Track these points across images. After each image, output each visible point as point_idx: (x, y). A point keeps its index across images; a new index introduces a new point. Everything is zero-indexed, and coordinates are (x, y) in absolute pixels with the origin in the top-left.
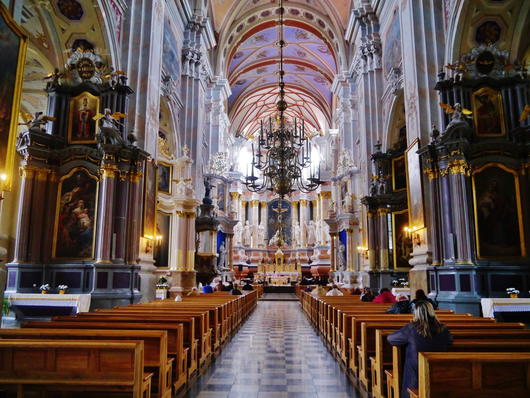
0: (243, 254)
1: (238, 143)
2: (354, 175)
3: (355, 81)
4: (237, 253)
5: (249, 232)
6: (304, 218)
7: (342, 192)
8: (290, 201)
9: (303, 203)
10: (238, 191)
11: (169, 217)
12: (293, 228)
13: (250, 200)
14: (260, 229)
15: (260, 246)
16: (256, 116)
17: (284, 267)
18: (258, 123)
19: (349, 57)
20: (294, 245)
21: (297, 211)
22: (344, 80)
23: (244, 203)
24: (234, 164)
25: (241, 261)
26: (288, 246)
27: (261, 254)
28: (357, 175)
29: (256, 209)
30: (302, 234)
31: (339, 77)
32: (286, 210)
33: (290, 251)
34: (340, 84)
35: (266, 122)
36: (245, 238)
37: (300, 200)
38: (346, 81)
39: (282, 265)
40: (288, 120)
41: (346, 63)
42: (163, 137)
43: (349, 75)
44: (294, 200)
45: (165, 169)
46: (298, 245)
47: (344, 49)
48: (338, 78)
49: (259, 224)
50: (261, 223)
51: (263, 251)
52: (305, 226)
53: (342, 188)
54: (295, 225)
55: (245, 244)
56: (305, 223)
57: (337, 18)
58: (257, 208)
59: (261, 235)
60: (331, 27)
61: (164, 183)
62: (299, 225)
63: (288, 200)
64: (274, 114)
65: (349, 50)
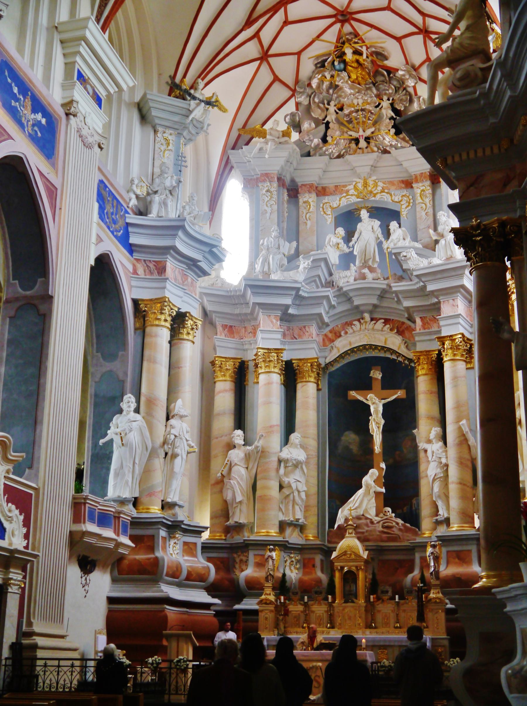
0: (195, 556)
1: (176, 118)
4: (152, 549)
5: (243, 471)
6: (458, 406)
8: (410, 355)
9: (455, 348)
10: (167, 294)
12: (422, 455)
13: (249, 356)
14: (286, 461)
15: (288, 531)
16: (249, 23)
17: (370, 608)
18: (276, 79)
20: (426, 524)
21: (435, 389)
23: (229, 365)
24: (156, 192)
25: (179, 585)
26: (407, 530)
27: (274, 554)
29: (269, 383)
30: (454, 472)
32: (400, 394)
33: (412, 549)
35: (310, 79)
36: (229, 497)
37: (442, 340)
39: (362, 601)
40: (386, 63)
44: (420, 347)
46: (438, 523)
49: (286, 441)
50: (294, 437)
51: (301, 549)
52: (466, 440)
54: (429, 441)
55: (231, 522)
56: (466, 429)
58: (276, 379)
59: (290, 486)
62: (444, 438)
63: (403, 350)
64: (332, 35)
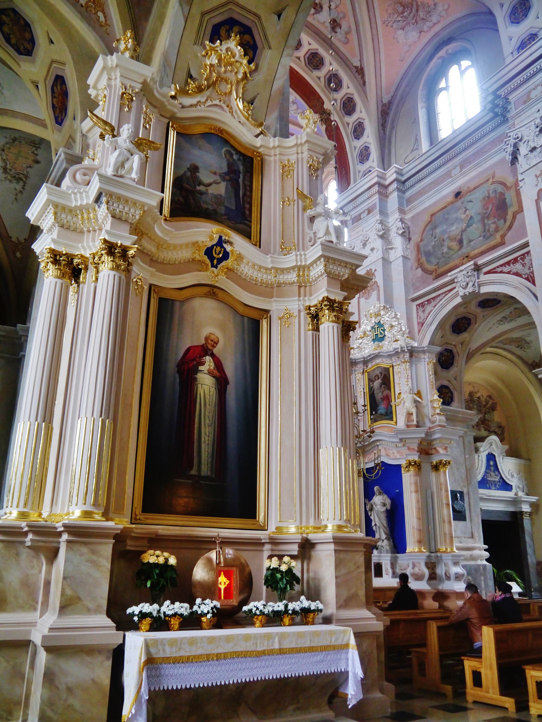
2: (415, 354)
3: (404, 192)
7: (371, 389)
11: (255, 326)
19: (384, 152)
22: (387, 183)
28: (422, 356)
31: (380, 174)
34: (376, 188)
38: (387, 187)
41: (381, 160)
42: (251, 53)
43: (402, 175)
45: (235, 157)
47: (378, 136)
48: (378, 176)
53: (370, 380)
57: (378, 78)
60: (357, 90)
61: (233, 200)
65: (384, 139)
